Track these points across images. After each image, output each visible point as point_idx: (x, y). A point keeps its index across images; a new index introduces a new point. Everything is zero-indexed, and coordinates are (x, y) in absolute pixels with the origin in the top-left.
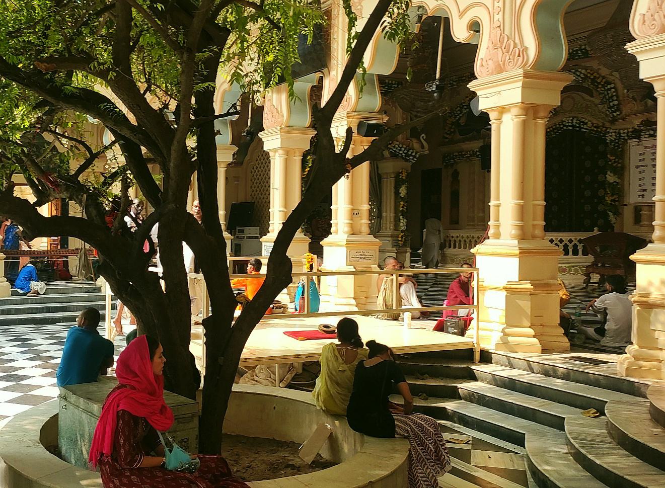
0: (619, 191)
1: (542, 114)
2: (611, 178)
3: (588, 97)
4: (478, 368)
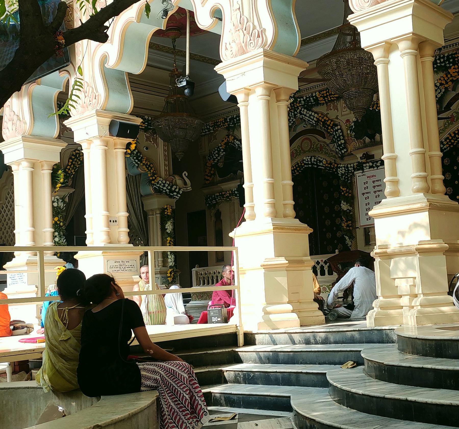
0: (351, 217)
1: (283, 97)
2: (344, 206)
3: (321, 139)
4: (243, 351)
